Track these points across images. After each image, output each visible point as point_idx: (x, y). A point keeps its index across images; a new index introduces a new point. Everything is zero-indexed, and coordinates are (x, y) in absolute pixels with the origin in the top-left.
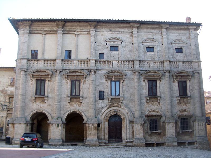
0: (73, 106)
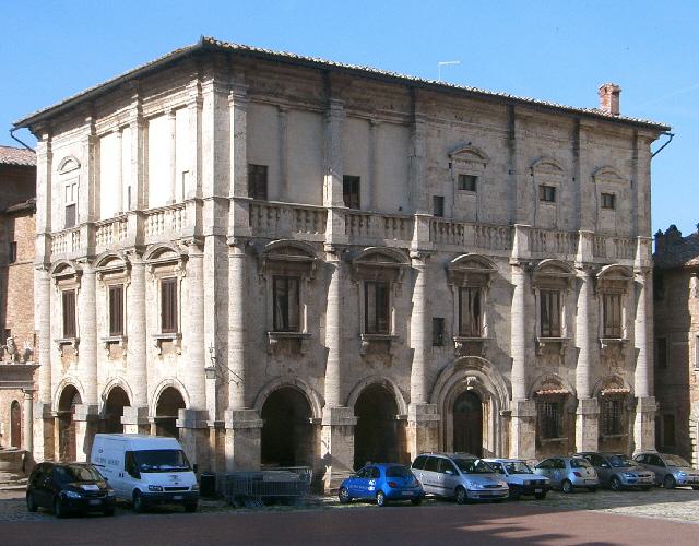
0: (372, 367)
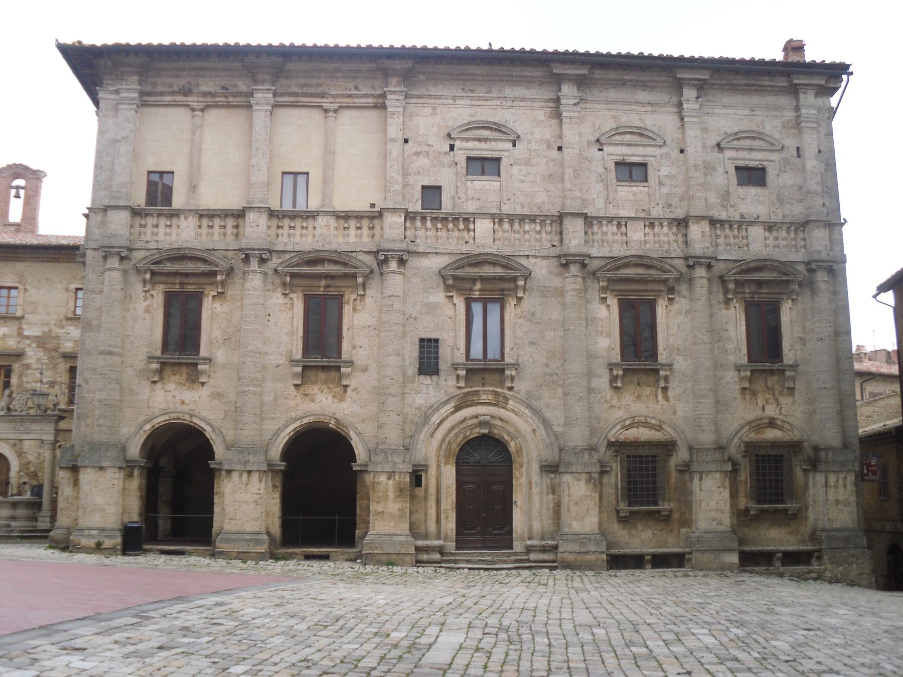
0: (313, 401)
